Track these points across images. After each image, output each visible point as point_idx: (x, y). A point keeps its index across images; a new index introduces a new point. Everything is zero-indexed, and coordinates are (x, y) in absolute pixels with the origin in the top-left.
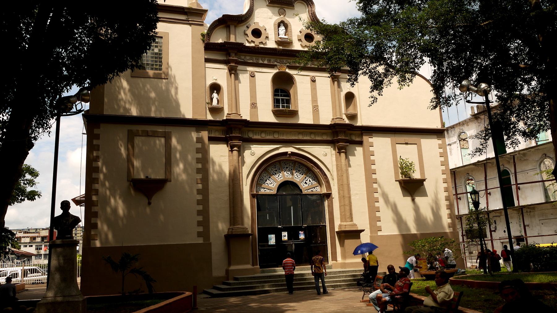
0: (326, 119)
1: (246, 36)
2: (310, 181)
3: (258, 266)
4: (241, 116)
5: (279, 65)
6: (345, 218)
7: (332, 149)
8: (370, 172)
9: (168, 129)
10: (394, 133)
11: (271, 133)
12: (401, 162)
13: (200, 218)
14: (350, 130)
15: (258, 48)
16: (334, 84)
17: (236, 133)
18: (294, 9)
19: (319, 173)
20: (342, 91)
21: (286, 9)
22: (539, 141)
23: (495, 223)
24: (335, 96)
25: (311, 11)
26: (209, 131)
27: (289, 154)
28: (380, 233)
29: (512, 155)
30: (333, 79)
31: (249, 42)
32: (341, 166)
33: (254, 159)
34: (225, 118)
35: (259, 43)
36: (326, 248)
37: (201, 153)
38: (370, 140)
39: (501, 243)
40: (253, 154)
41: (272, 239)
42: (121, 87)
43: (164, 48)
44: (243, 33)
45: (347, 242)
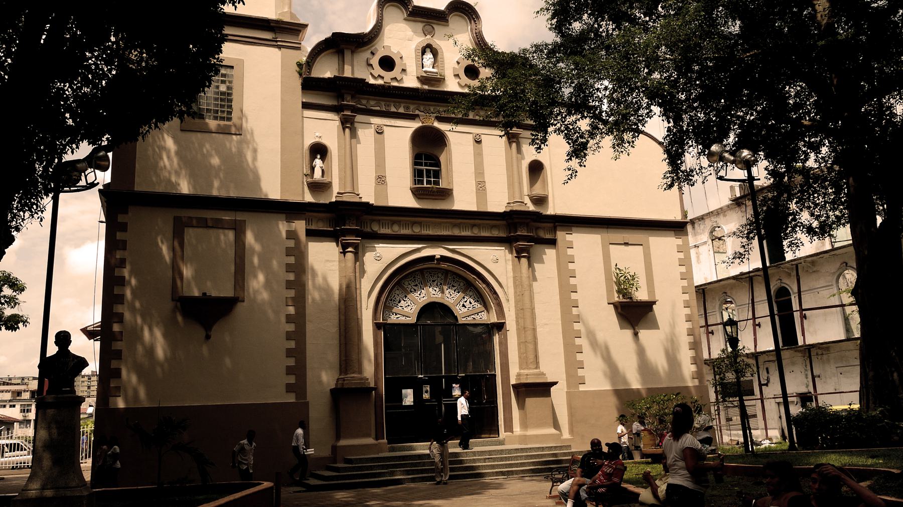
0: (498, 203)
1: (370, 68)
2: (471, 303)
3: (385, 441)
4: (360, 196)
5: (423, 116)
6: (526, 363)
7: (507, 251)
8: (567, 291)
9: (240, 216)
10: (607, 226)
11: (408, 224)
12: (617, 274)
13: (291, 362)
14: (535, 221)
15: (389, 86)
16: (511, 147)
17: (352, 223)
18: (448, 26)
19: (485, 290)
20: (523, 158)
21: (435, 26)
22: (836, 242)
23: (768, 372)
24: (512, 166)
25: (476, 29)
26: (307, 220)
27: (438, 259)
28: (582, 388)
29: (793, 263)
30: (509, 139)
31: (375, 76)
32: (521, 280)
33: (381, 266)
34: (334, 200)
35: (391, 79)
36: (496, 411)
37: (294, 256)
38: (569, 237)
39: (777, 404)
40: (378, 259)
41: (408, 397)
42: (163, 148)
43: (235, 85)
44: (365, 63)
45: (530, 402)
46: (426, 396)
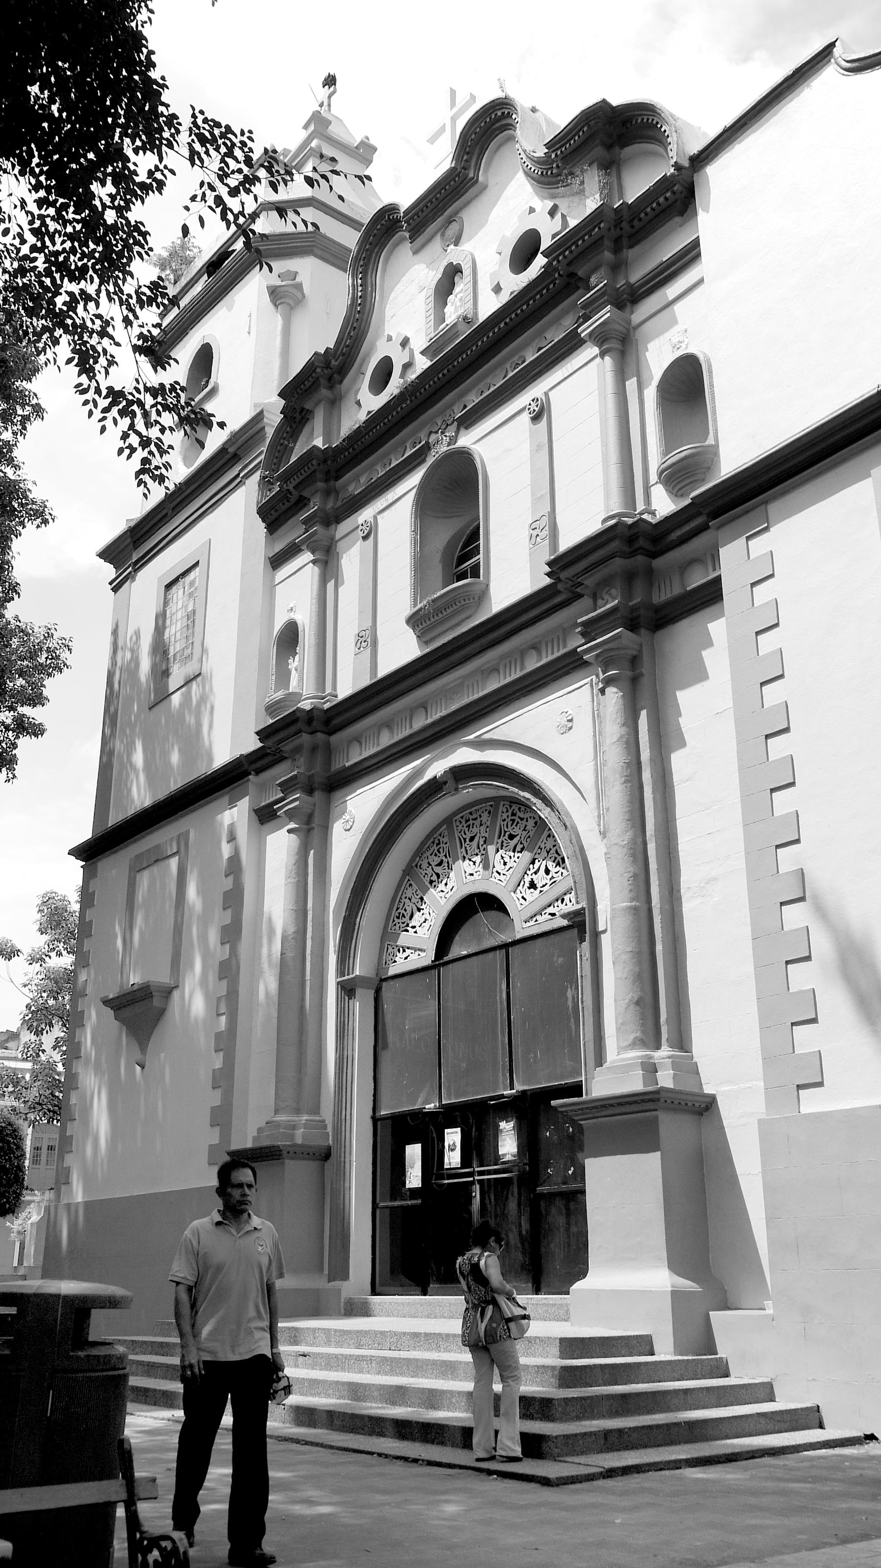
2: (547, 871)
46: (453, 1159)
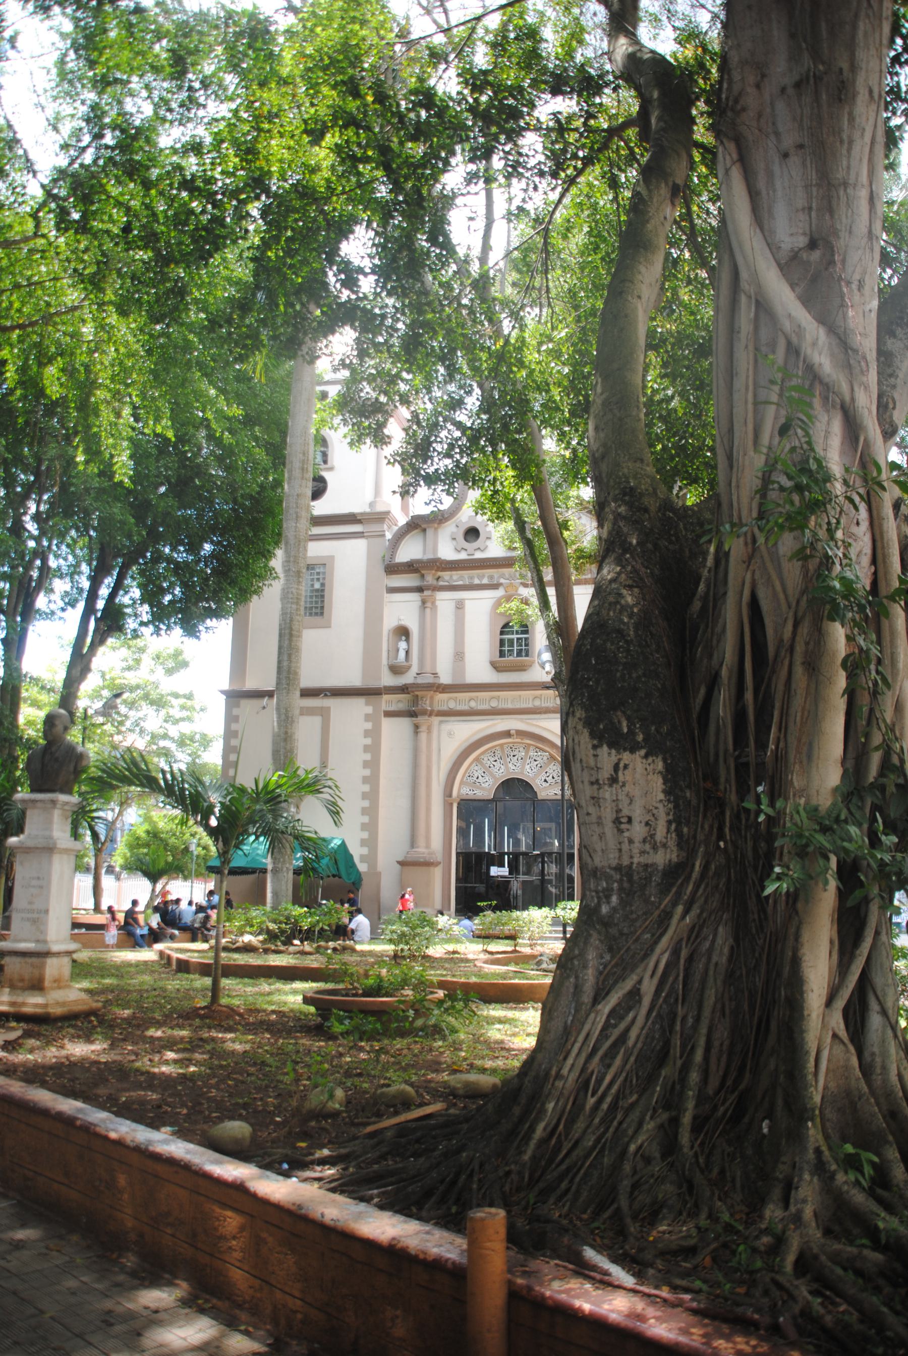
43: (327, 582)
